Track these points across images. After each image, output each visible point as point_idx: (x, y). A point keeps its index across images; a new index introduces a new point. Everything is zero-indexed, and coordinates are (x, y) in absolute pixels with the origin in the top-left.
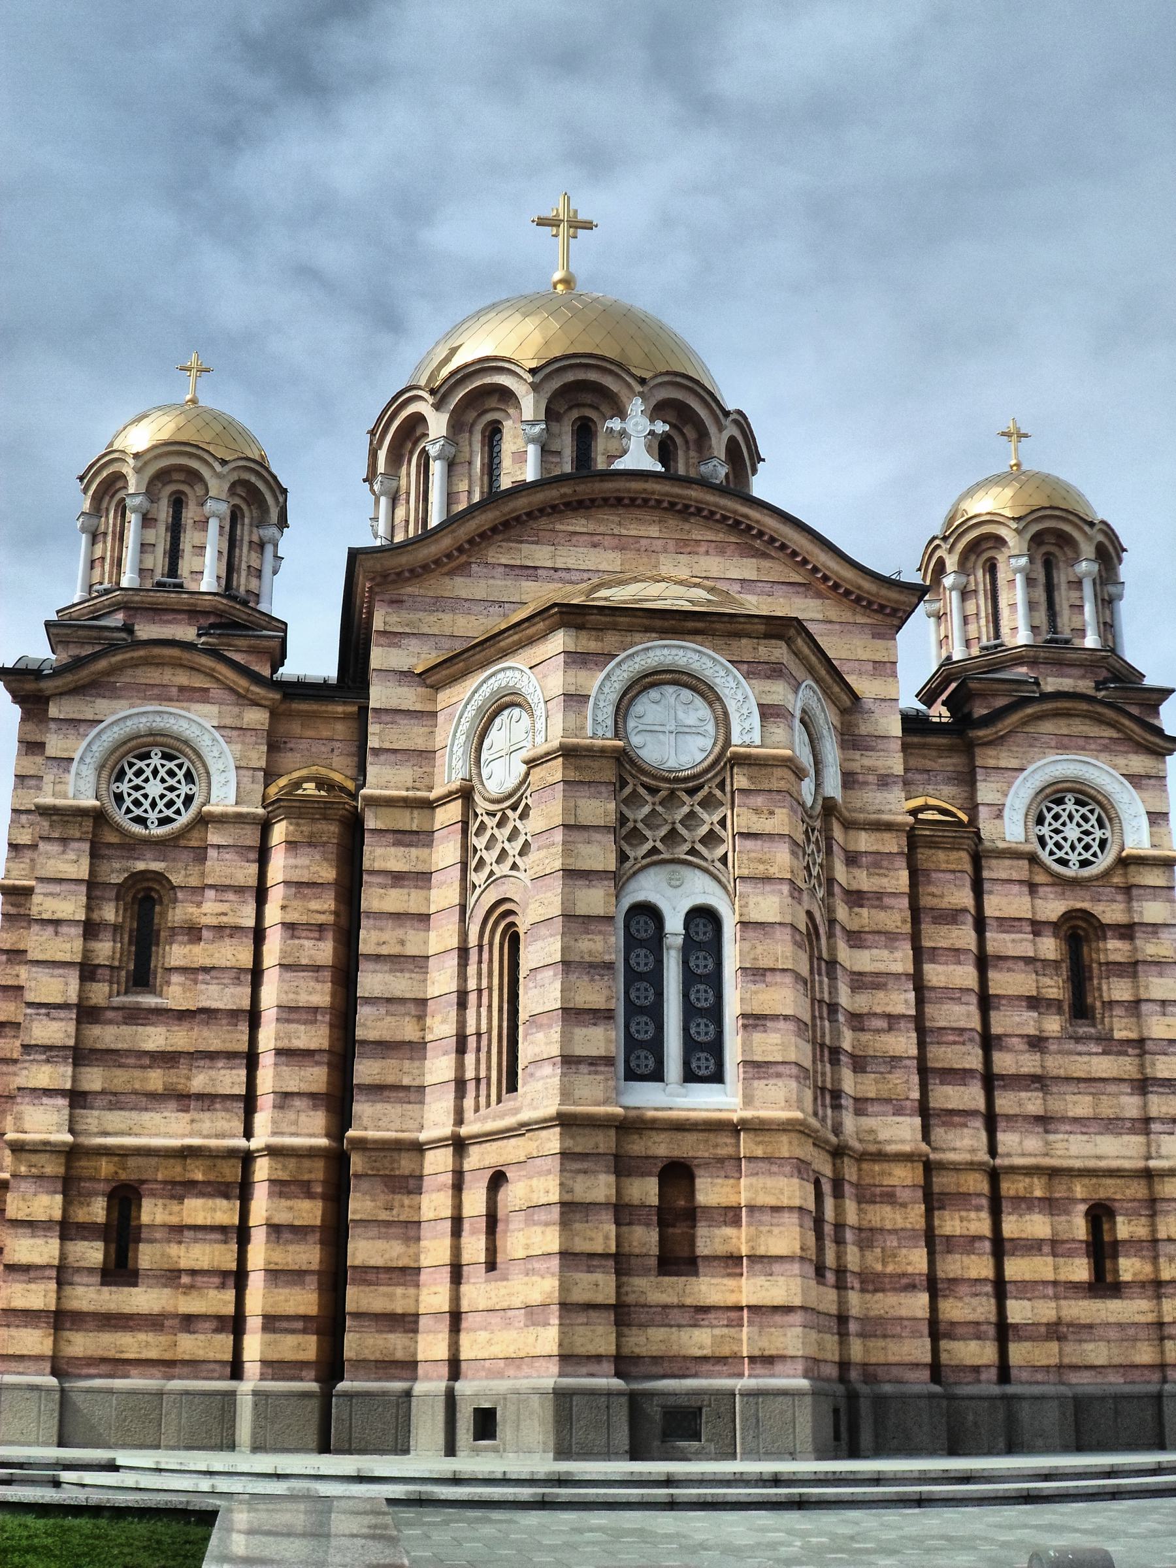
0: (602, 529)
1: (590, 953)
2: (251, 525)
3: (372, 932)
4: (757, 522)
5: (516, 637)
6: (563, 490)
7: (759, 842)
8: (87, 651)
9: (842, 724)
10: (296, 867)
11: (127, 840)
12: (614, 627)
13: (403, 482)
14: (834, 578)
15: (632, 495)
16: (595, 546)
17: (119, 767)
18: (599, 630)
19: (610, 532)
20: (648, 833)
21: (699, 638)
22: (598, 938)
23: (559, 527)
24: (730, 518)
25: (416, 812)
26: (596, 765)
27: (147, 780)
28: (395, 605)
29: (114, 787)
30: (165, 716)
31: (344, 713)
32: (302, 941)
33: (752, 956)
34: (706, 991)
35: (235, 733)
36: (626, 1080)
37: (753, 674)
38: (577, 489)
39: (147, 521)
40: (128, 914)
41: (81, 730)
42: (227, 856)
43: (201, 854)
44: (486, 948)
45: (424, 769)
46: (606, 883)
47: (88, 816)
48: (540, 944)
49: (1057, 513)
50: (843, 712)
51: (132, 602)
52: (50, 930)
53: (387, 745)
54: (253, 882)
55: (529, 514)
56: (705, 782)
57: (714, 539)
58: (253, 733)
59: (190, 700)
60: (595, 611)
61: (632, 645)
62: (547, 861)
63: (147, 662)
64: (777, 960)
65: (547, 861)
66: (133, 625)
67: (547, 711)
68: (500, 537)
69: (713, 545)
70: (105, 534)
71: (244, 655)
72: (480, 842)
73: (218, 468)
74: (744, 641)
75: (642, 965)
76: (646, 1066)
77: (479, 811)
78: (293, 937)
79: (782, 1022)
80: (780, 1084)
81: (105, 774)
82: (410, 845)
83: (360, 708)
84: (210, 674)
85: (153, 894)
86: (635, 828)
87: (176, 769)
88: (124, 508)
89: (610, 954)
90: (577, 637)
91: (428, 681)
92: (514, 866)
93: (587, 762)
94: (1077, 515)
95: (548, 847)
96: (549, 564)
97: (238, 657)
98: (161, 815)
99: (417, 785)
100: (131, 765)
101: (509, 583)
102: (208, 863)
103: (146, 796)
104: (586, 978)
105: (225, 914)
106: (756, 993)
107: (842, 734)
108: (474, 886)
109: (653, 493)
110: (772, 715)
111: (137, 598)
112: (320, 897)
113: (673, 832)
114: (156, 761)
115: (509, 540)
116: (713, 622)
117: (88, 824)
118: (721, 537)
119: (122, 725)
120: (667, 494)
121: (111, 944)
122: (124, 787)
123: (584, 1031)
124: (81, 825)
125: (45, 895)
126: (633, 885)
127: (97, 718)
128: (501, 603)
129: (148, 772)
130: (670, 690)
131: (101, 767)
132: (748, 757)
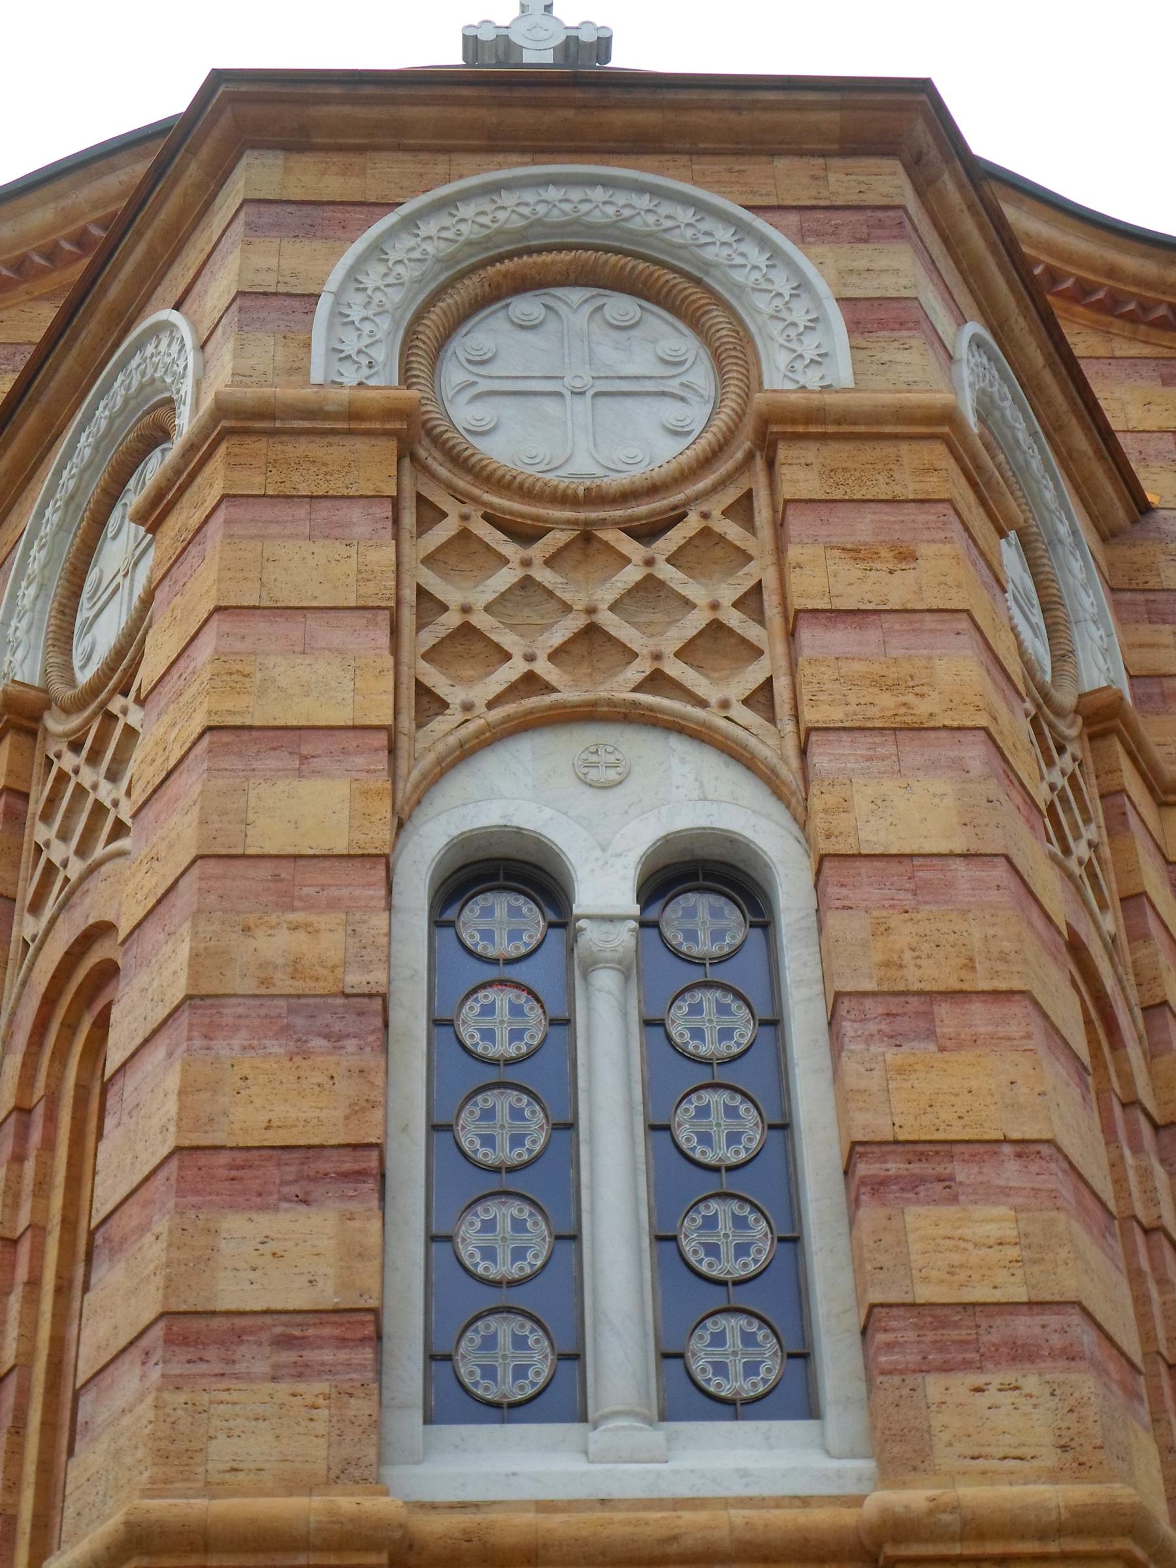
1: (296, 968)
7: (872, 636)
9: (1111, 565)
20: (507, 640)
21: (650, 160)
26: (334, 452)
33: (878, 957)
34: (731, 1112)
36: (428, 1420)
37: (819, 234)
46: (359, 761)
50: (1108, 535)
56: (688, 502)
64: (970, 965)
74: (782, 164)
75: (502, 1035)
76: (520, 1372)
79: (1013, 1166)
80: (1031, 1383)
86: (467, 631)
89: (366, 966)
104: (276, 1047)
106: (900, 1071)
107: (1112, 590)
110: (882, 324)
113: (592, 633)
123: (265, 1223)
130: (575, 295)
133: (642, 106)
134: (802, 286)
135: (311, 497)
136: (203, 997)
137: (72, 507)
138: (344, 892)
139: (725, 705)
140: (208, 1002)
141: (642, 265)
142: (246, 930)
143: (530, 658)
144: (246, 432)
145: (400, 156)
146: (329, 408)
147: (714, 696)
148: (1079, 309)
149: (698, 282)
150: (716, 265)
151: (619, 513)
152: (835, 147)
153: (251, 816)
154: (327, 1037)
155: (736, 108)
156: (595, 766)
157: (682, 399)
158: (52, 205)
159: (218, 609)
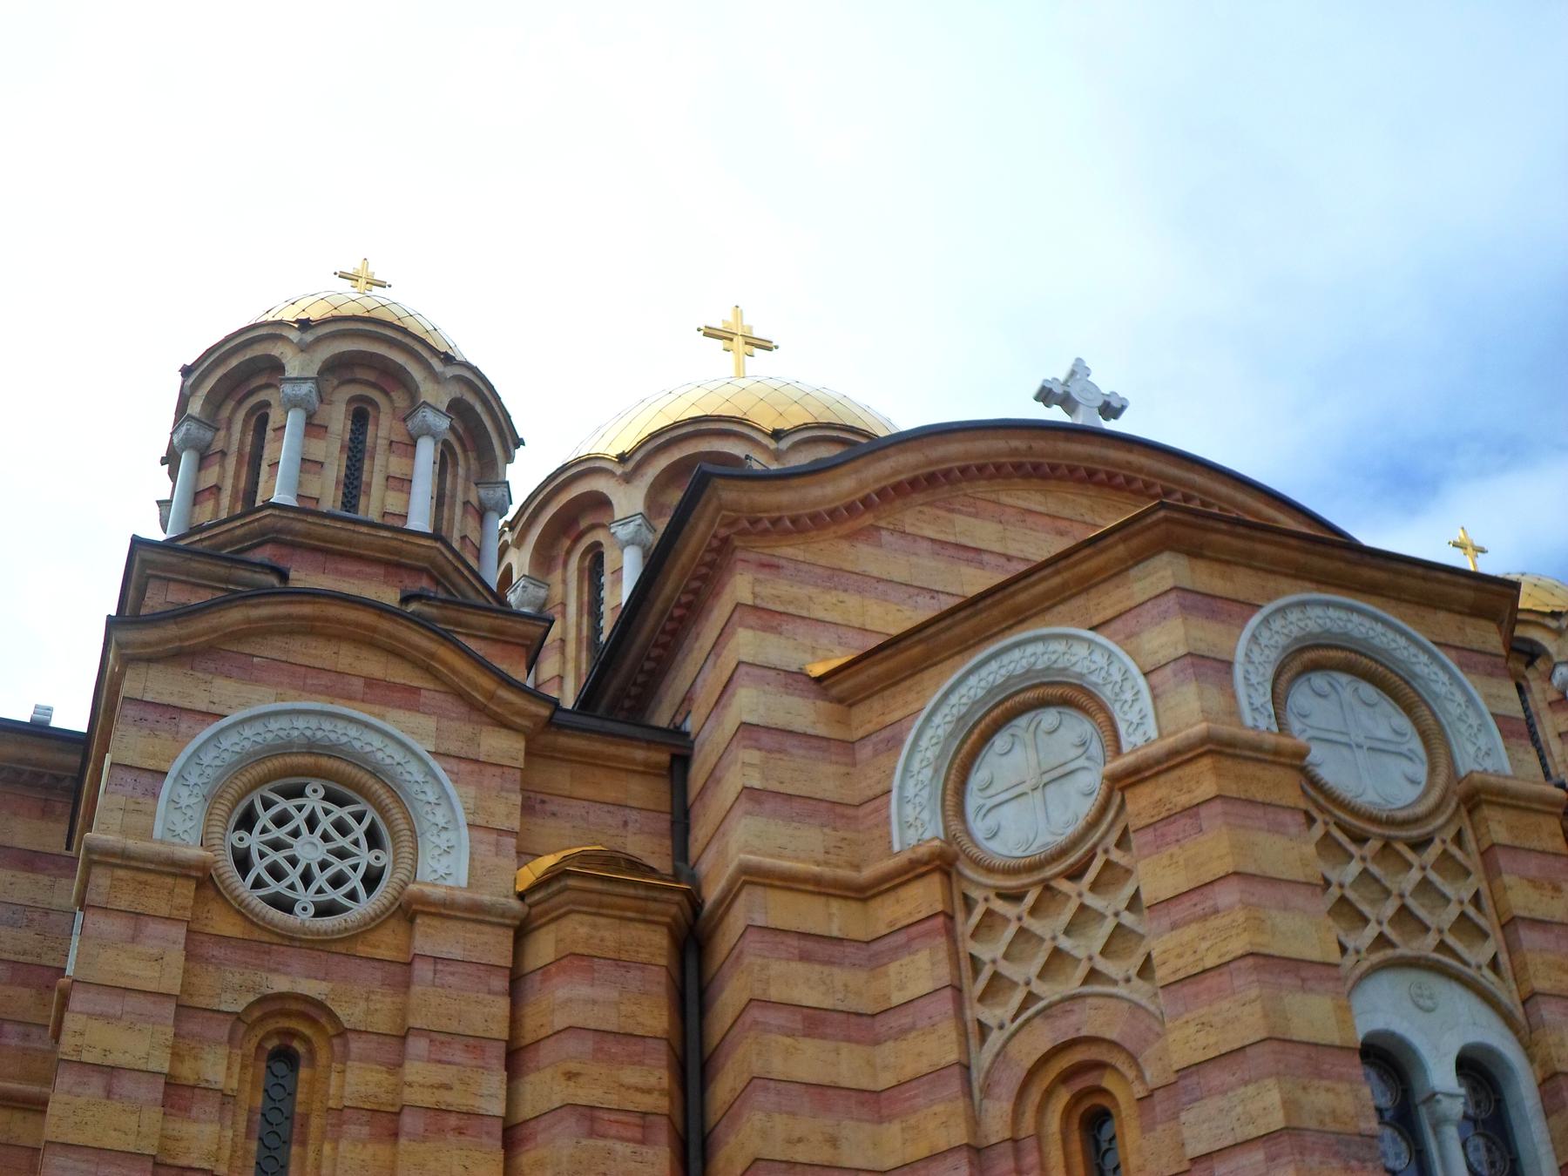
0: (1067, 512)
2: (467, 479)
3: (777, 1117)
5: (1056, 581)
10: (594, 1002)
11: (257, 934)
12: (1248, 561)
13: (557, 590)
17: (244, 803)
18: (1227, 560)
19: (1080, 518)
22: (1342, 1087)
23: (1004, 499)
25: (835, 905)
26: (1270, 774)
27: (296, 833)
28: (767, 570)
29: (234, 838)
30: (341, 725)
31: (646, 764)
32: (609, 1143)
35: (465, 767)
39: (313, 427)
40: (249, 1077)
41: (183, 727)
42: (450, 979)
43: (402, 972)
44: (1030, 1144)
45: (841, 834)
47: (188, 877)
48: (1212, 1105)
51: (290, 532)
52: (96, 1084)
53: (774, 786)
54: (500, 1030)
55: (964, 471)
58: (498, 771)
59: (386, 703)
60: (1223, 526)
61: (1278, 594)
62: (1204, 945)
63: (310, 629)
65: (1204, 945)
66: (289, 569)
67: (1152, 688)
68: (919, 497)
70: (223, 454)
72: (990, 951)
73: (437, 364)
74: (1442, 616)
77: (975, 894)
78: (592, 1133)
81: (221, 809)
82: (829, 962)
83: (674, 757)
84: (425, 666)
85: (297, 1045)
86: (1343, 900)
87: (352, 821)
88: (263, 421)
90: (1193, 570)
91: (834, 692)
92: (1093, 975)
93: (1250, 769)
95: (1204, 917)
96: (997, 548)
97: (472, 644)
98: (321, 898)
99: (832, 858)
100: (267, 804)
102: (416, 989)
103: (293, 861)
104: (1335, 1163)
105: (448, 1087)
108: (984, 1030)
109: (1140, 470)
111: (298, 526)
112: (641, 1063)
114: (314, 801)
117: (186, 891)
119: (258, 727)
121: (216, 1128)
122: (253, 841)
124: (171, 892)
125: (90, 1015)
126: (1360, 1002)
127: (214, 709)
129: (299, 820)
130: (1344, 679)
131: (212, 799)
132: (1502, 792)
133: (1380, 568)
134: (1470, 700)
135: (1263, 804)
136: (1294, 1129)
137: (961, 723)
138: (1344, 1070)
139: (1479, 967)
140: (1296, 1132)
141: (1380, 669)
142: (1304, 1088)
143: (1380, 923)
144: (1220, 753)
145: (1251, 572)
146: (1266, 747)
147: (1473, 962)
149: (1407, 683)
150: (1421, 678)
151: (1403, 834)
152: (1467, 610)
153: (1289, 1016)
154: (1358, 1160)
155: (1424, 578)
156: (1421, 996)
157: (1411, 759)
158: (854, 476)
159: (1236, 873)
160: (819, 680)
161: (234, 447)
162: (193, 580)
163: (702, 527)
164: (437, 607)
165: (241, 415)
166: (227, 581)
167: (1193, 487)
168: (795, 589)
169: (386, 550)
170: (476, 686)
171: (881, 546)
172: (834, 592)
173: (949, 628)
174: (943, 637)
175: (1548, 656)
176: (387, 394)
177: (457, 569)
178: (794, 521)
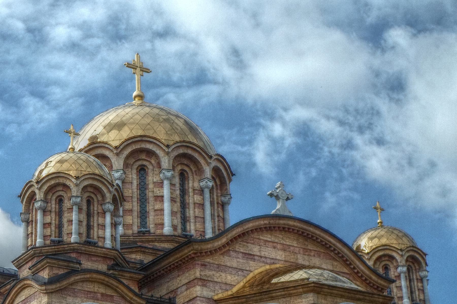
0: (276, 241)
4: (334, 245)
5: (283, 293)
6: (266, 222)
8: (61, 272)
14: (361, 272)
15: (289, 227)
16: (274, 248)
24: (324, 241)
38: (271, 222)
49: (414, 249)
57: (316, 249)
69: (316, 252)
71: (127, 281)
73: (110, 187)
94: (422, 251)
96: (258, 254)
97: (125, 282)
101: (245, 261)
109: (297, 227)
111: (83, 248)
115: (242, 241)
116: (366, 296)
118: (318, 249)
120: (302, 228)
128: (242, 270)
148: (364, 283)
160: (215, 301)
161: (54, 210)
162: (59, 266)
163: (186, 251)
164: (117, 272)
165: (54, 198)
166: (68, 266)
167: (310, 231)
168: (210, 273)
169: (104, 254)
170: (128, 296)
171: (230, 256)
172: (219, 272)
173: (254, 297)
174: (251, 299)
175: (397, 261)
176: (96, 195)
177: (119, 257)
178: (210, 252)
